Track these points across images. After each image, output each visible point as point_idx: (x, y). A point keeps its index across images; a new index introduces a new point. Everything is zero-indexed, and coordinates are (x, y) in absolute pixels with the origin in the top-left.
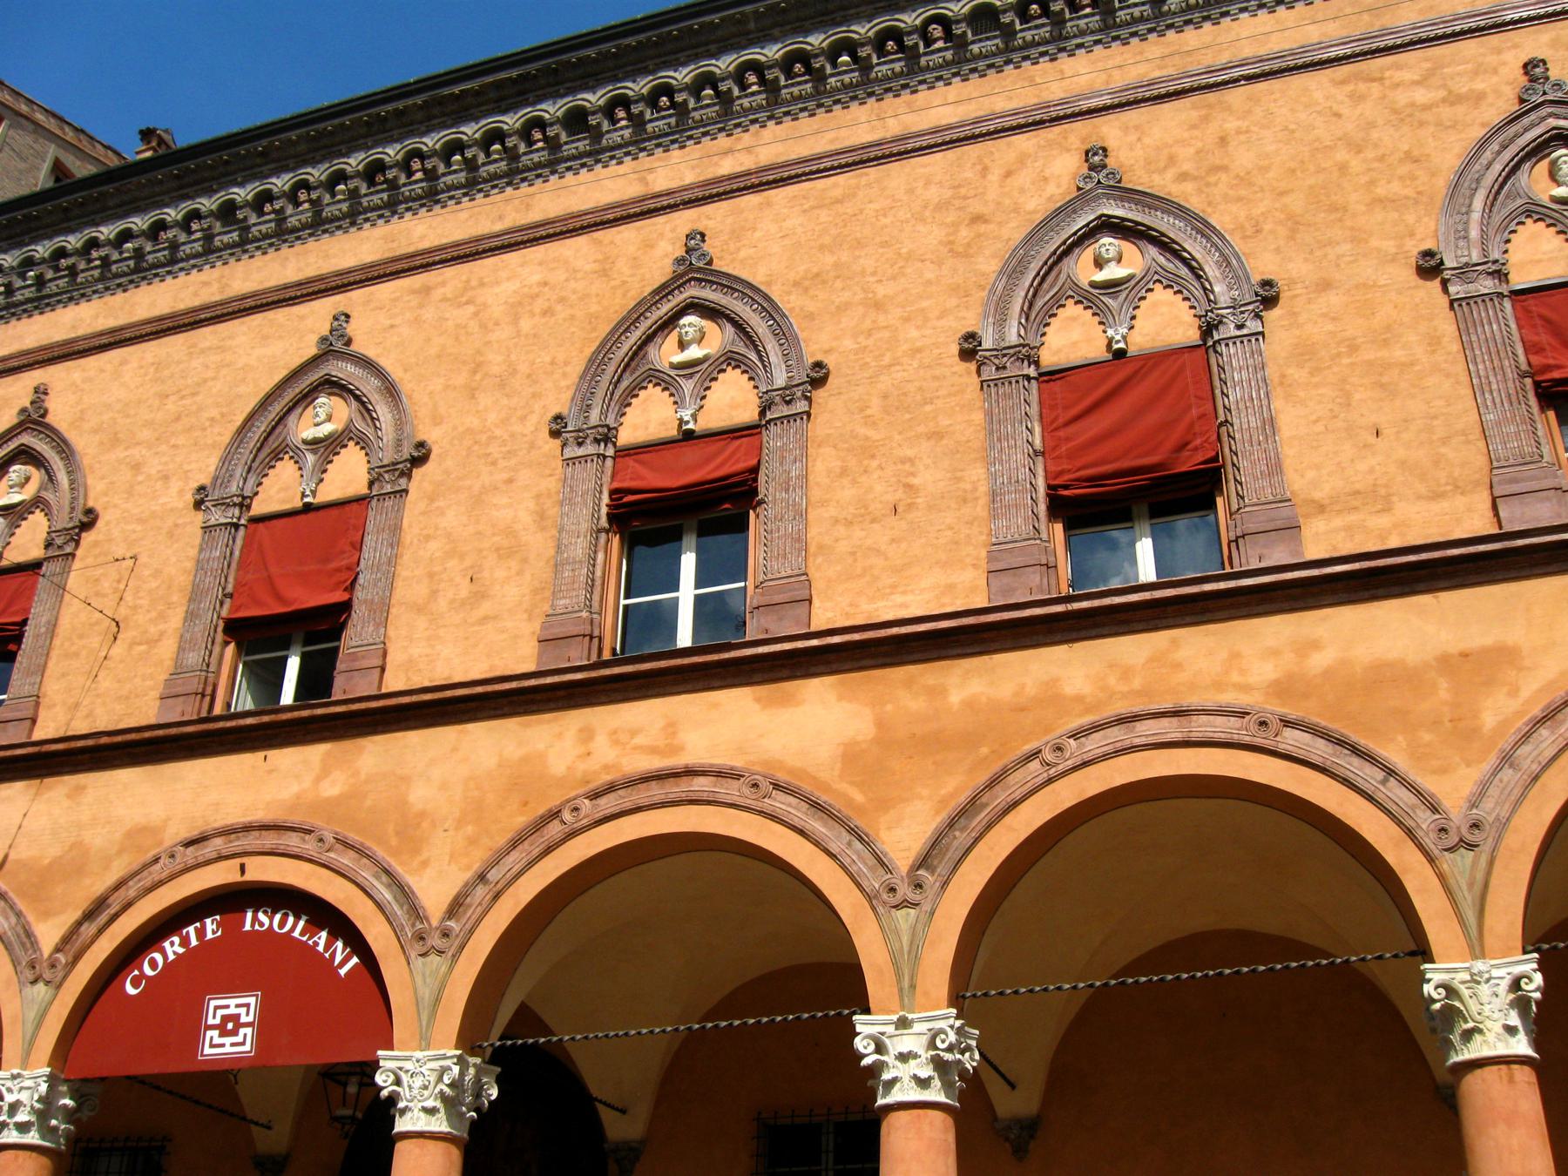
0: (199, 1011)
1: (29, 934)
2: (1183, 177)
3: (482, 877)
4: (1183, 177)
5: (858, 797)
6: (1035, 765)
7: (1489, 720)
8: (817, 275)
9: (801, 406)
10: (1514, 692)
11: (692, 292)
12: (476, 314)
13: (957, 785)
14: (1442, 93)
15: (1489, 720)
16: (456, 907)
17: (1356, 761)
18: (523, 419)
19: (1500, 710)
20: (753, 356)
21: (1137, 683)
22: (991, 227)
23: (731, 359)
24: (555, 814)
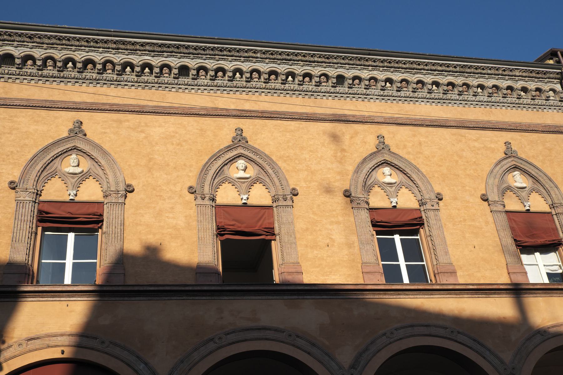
2: (409, 153)
3: (182, 362)
4: (409, 153)
8: (288, 157)
9: (289, 203)
11: (240, 151)
12: (146, 137)
14: (482, 146)
18: (175, 185)
20: (268, 180)
22: (349, 154)
23: (257, 180)
24: (212, 340)
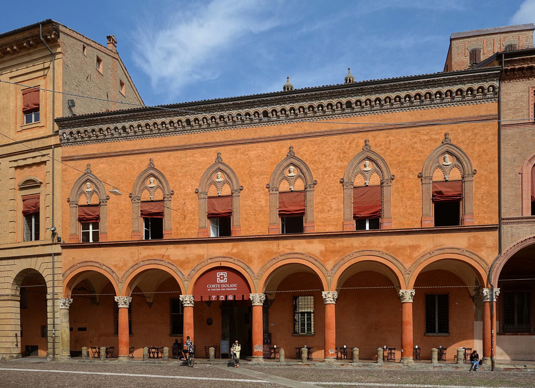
7: (414, 256)
10: (419, 252)
12: (248, 158)
15: (414, 256)
19: (416, 255)
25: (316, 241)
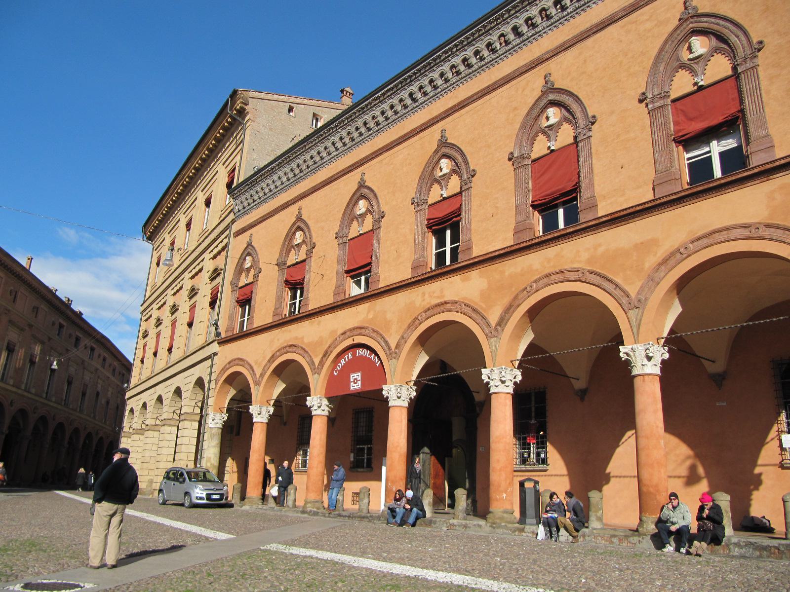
0: (349, 377)
1: (313, 362)
5: (484, 306)
6: (525, 292)
13: (506, 301)
16: (398, 346)
17: (608, 283)
21: (552, 264)
25: (474, 274)
